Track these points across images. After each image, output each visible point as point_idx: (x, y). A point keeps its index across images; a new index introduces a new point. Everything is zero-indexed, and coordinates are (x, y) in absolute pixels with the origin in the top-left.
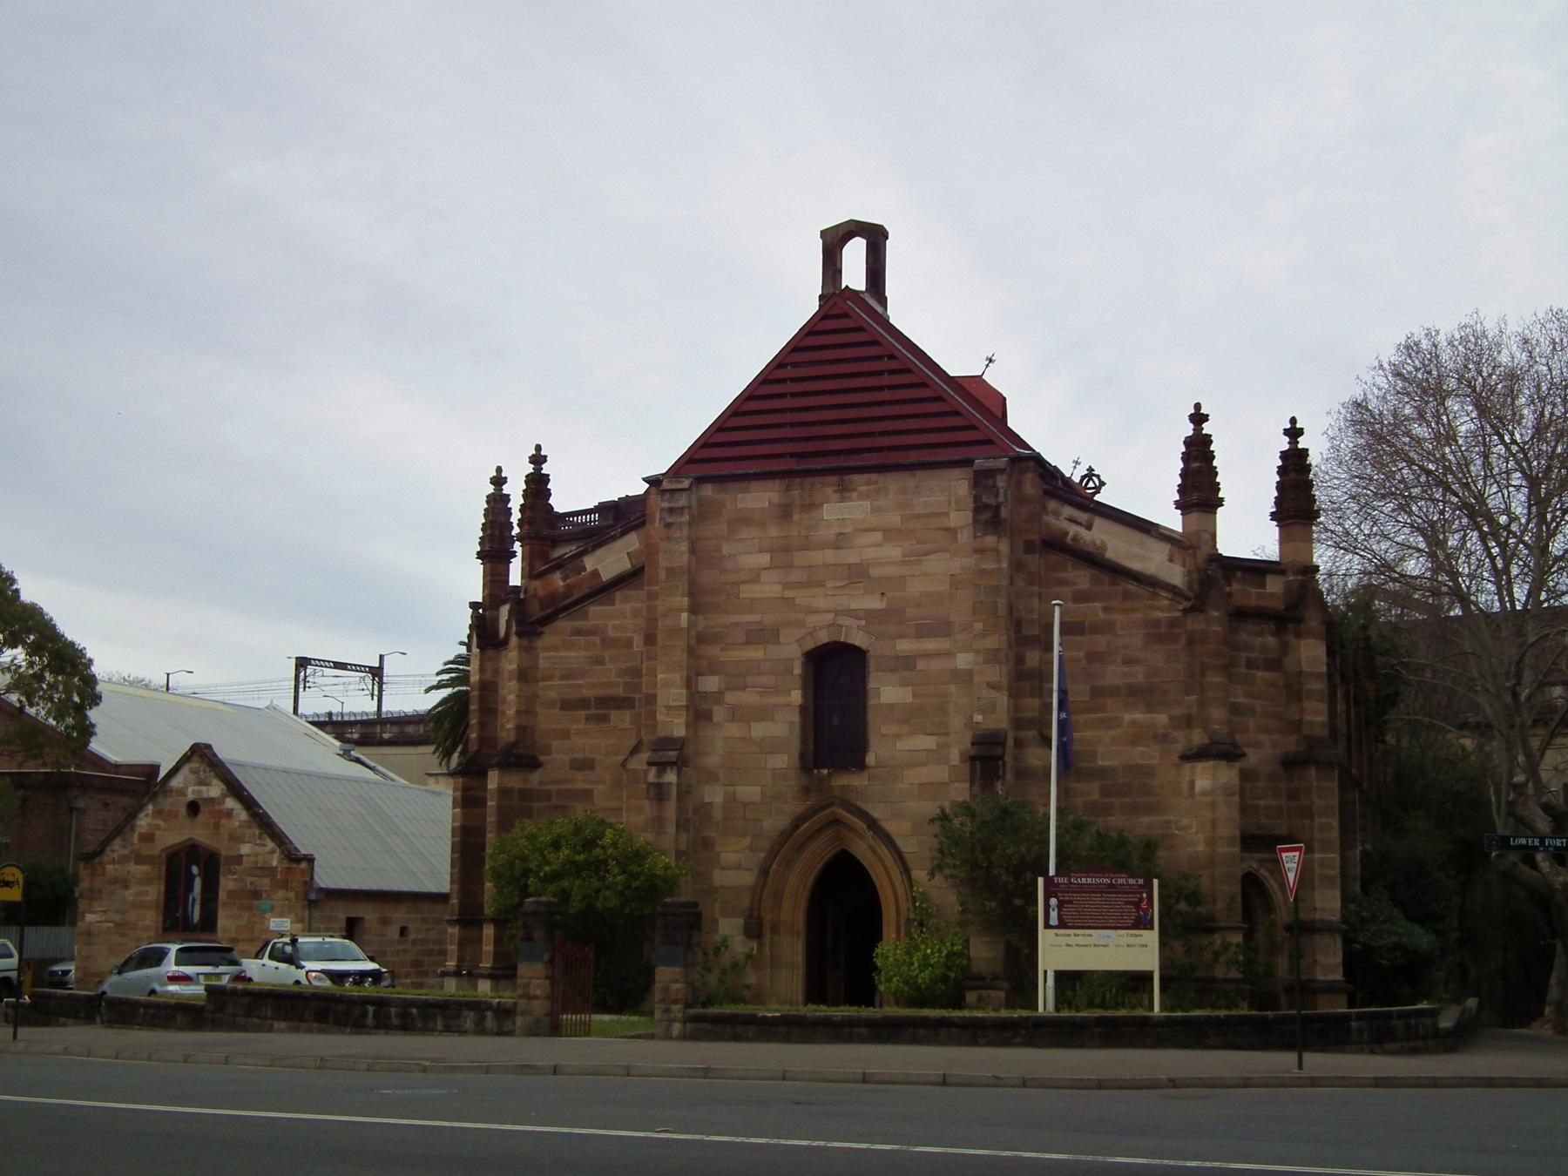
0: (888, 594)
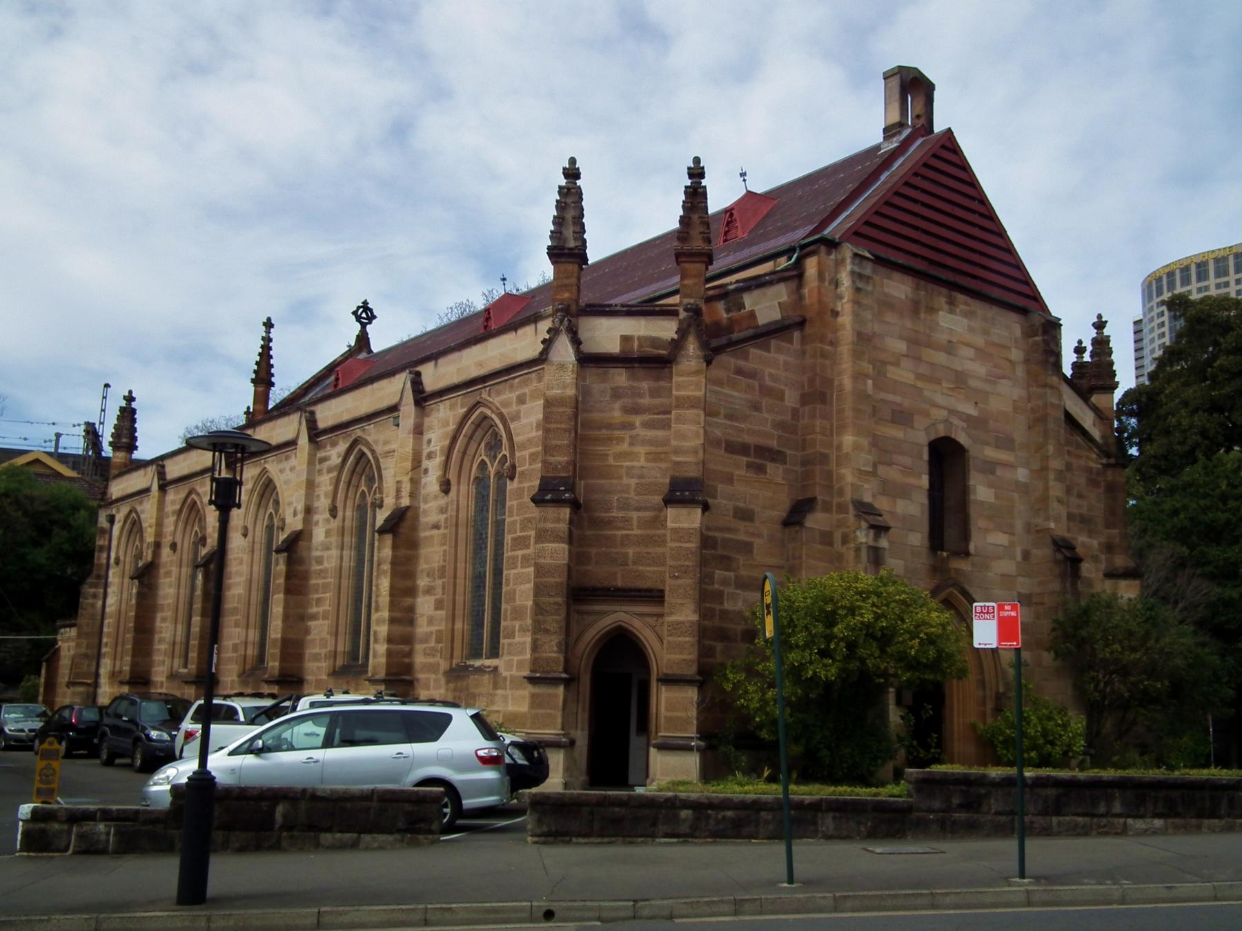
0: (979, 405)
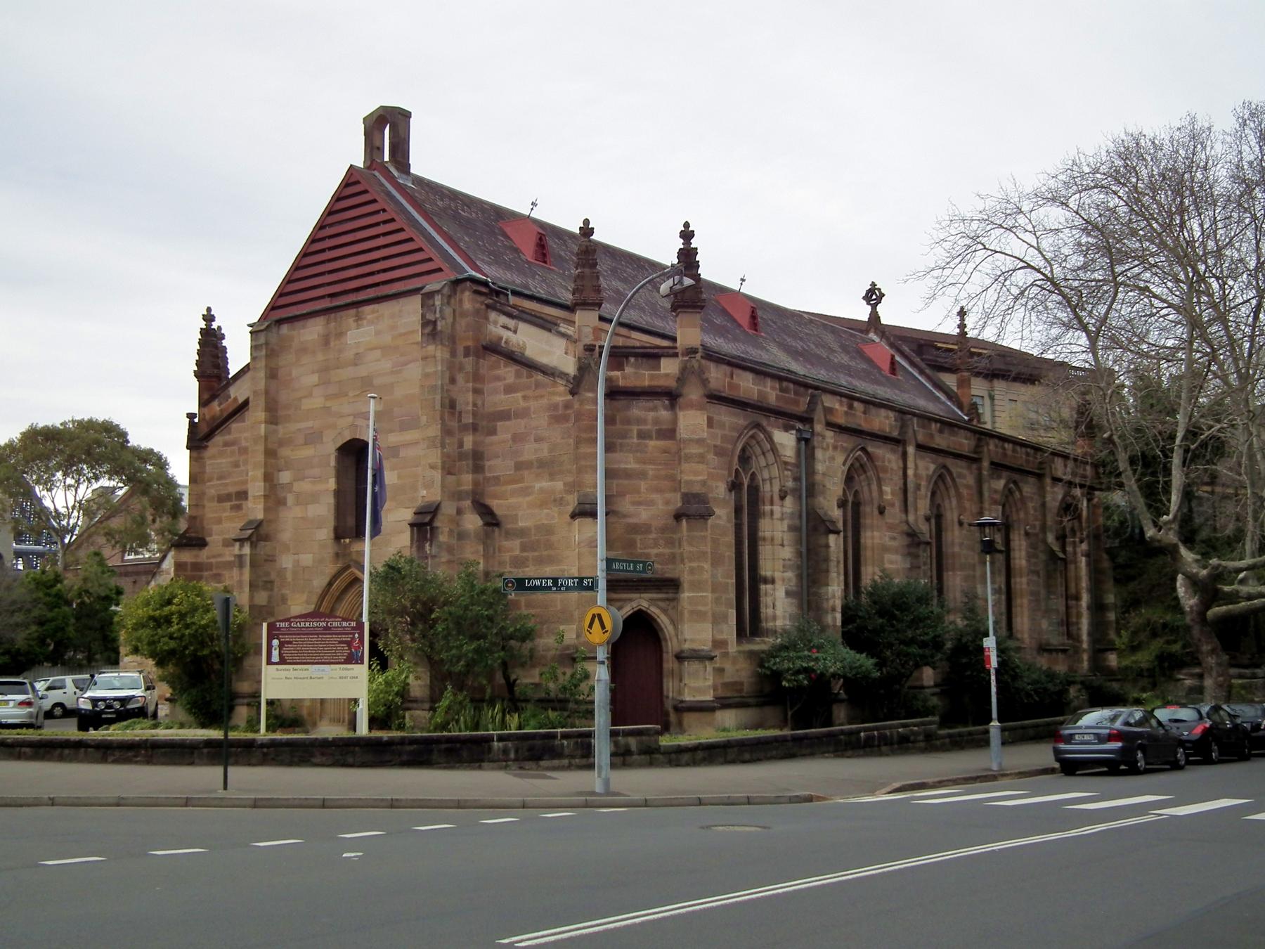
0: (384, 398)
